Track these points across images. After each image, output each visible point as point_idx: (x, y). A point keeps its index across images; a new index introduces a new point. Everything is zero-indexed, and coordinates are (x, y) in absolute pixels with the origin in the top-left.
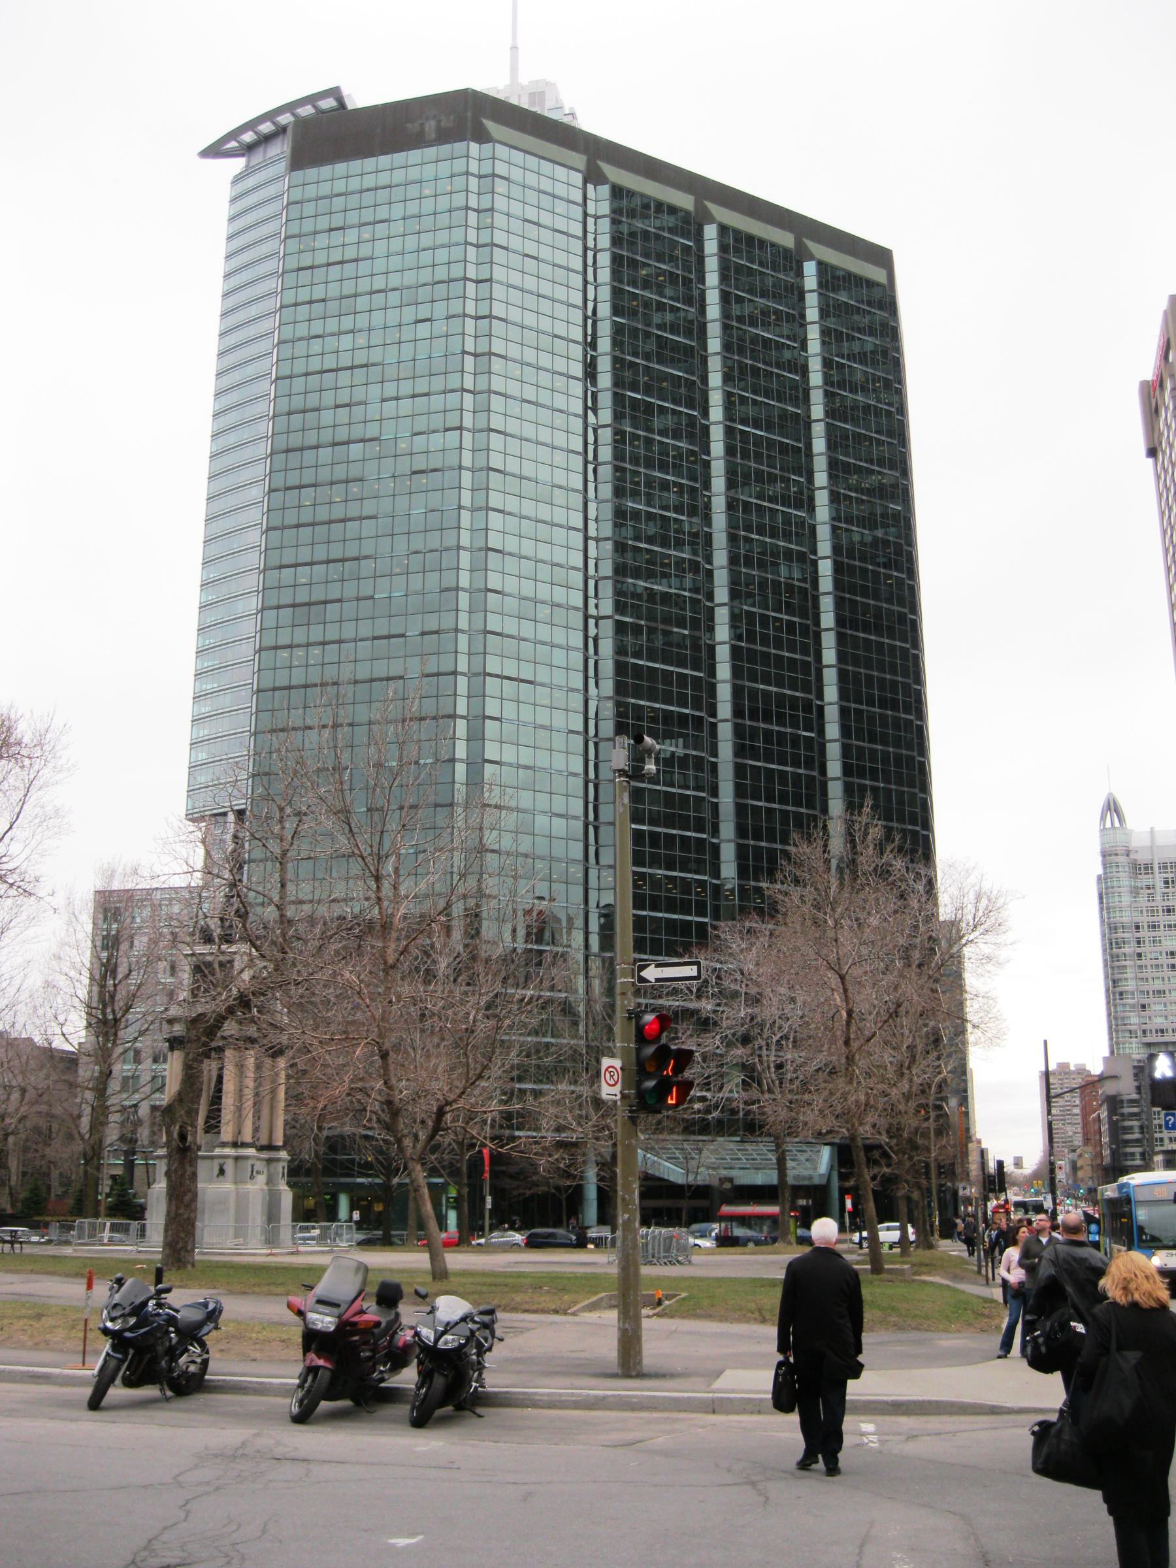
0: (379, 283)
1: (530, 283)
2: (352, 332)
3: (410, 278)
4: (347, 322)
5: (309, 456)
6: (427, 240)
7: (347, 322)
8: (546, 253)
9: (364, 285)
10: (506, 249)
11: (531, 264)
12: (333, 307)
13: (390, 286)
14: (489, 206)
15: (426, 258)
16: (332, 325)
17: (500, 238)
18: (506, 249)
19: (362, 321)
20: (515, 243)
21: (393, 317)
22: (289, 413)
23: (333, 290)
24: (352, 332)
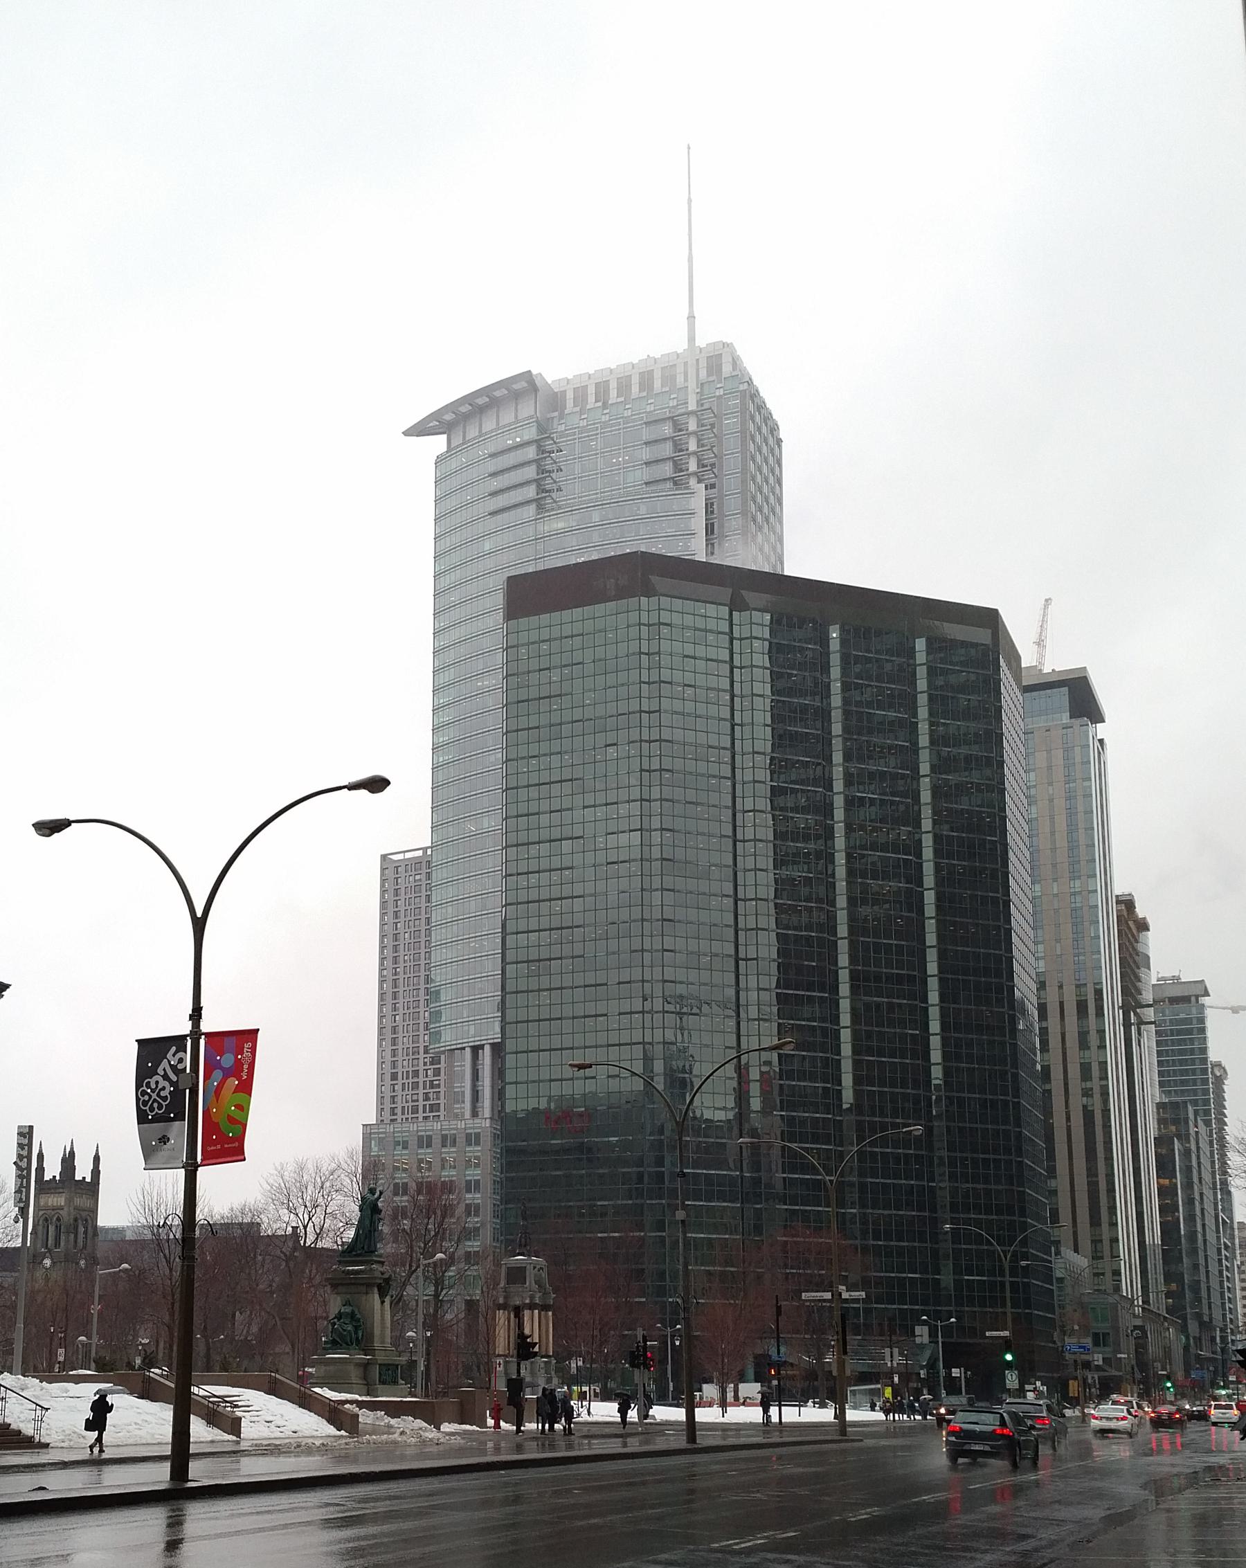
0: (578, 714)
1: (689, 707)
2: (560, 753)
3: (600, 711)
4: (556, 746)
5: (534, 850)
6: (611, 680)
7: (556, 746)
8: (701, 680)
9: (567, 716)
10: (670, 683)
11: (689, 691)
12: (544, 732)
13: (586, 717)
14: (657, 650)
15: (611, 693)
16: (545, 747)
17: (666, 675)
18: (670, 683)
19: (566, 743)
20: (678, 676)
21: (589, 740)
22: (517, 816)
23: (544, 720)
24: (560, 753)
